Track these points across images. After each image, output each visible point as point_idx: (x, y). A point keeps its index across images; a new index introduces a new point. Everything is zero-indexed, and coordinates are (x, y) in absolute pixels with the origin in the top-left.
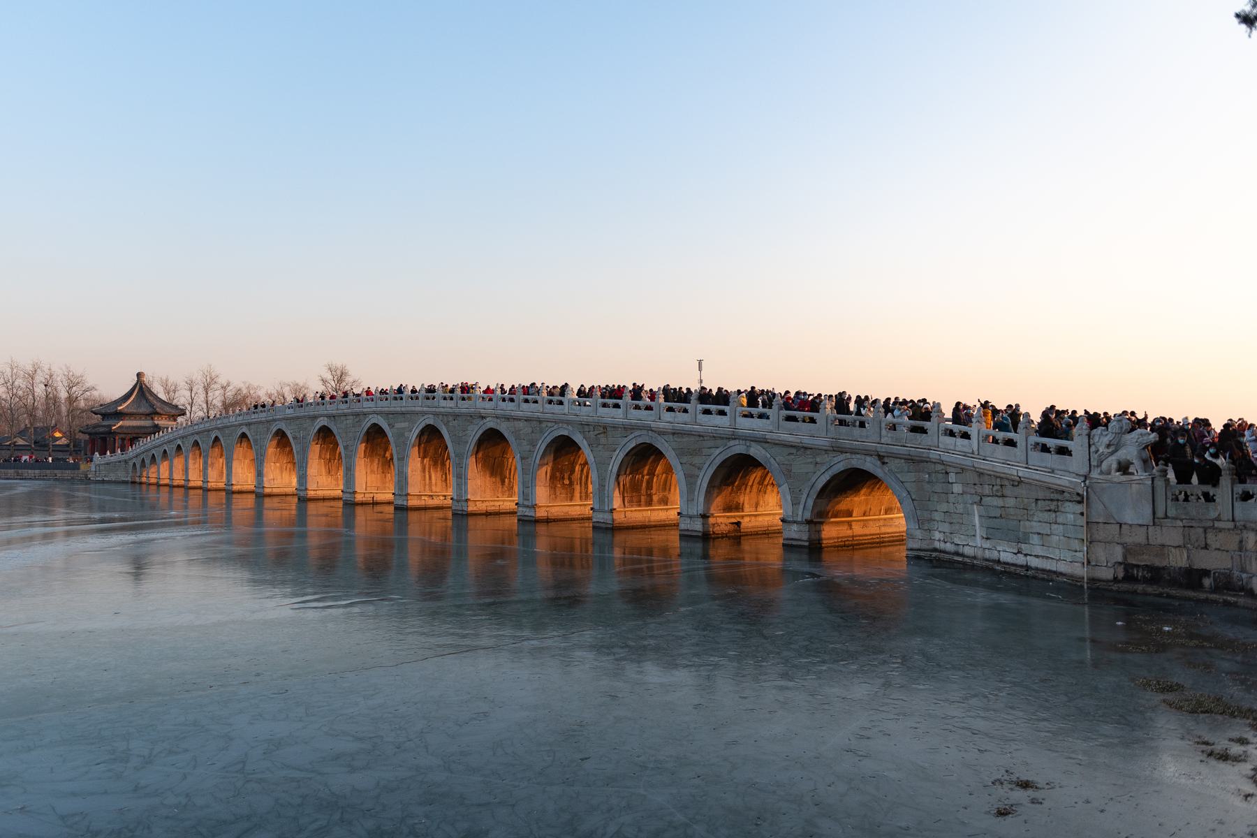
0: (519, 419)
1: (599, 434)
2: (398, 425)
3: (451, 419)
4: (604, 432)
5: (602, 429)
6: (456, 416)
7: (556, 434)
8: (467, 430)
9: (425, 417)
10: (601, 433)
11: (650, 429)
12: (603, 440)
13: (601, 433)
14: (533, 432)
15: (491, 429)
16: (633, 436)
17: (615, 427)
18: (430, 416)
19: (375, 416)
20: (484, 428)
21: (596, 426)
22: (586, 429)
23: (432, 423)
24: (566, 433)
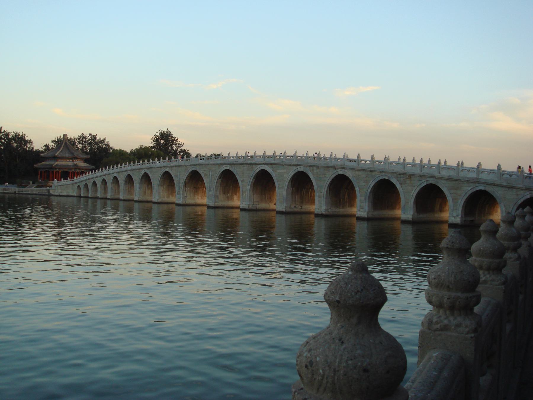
0: (358, 170)
1: (406, 179)
2: (278, 171)
3: (315, 168)
4: (409, 178)
5: (407, 176)
6: (318, 167)
7: (381, 178)
8: (326, 174)
9: (298, 167)
10: (407, 179)
11: (435, 177)
12: (408, 181)
13: (407, 179)
14: (367, 177)
15: (341, 175)
16: (425, 180)
17: (415, 176)
18: (301, 167)
19: (264, 165)
20: (337, 174)
21: (405, 174)
22: (399, 176)
23: (303, 171)
24: (386, 178)
